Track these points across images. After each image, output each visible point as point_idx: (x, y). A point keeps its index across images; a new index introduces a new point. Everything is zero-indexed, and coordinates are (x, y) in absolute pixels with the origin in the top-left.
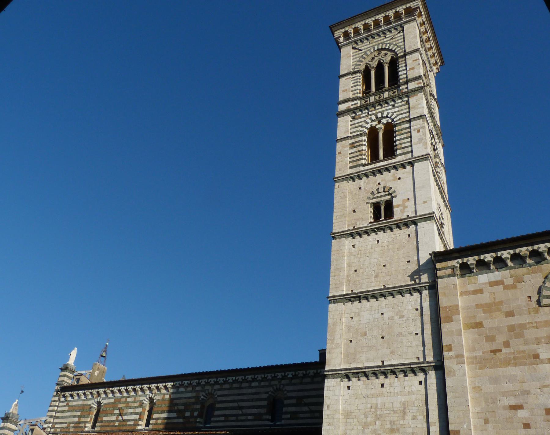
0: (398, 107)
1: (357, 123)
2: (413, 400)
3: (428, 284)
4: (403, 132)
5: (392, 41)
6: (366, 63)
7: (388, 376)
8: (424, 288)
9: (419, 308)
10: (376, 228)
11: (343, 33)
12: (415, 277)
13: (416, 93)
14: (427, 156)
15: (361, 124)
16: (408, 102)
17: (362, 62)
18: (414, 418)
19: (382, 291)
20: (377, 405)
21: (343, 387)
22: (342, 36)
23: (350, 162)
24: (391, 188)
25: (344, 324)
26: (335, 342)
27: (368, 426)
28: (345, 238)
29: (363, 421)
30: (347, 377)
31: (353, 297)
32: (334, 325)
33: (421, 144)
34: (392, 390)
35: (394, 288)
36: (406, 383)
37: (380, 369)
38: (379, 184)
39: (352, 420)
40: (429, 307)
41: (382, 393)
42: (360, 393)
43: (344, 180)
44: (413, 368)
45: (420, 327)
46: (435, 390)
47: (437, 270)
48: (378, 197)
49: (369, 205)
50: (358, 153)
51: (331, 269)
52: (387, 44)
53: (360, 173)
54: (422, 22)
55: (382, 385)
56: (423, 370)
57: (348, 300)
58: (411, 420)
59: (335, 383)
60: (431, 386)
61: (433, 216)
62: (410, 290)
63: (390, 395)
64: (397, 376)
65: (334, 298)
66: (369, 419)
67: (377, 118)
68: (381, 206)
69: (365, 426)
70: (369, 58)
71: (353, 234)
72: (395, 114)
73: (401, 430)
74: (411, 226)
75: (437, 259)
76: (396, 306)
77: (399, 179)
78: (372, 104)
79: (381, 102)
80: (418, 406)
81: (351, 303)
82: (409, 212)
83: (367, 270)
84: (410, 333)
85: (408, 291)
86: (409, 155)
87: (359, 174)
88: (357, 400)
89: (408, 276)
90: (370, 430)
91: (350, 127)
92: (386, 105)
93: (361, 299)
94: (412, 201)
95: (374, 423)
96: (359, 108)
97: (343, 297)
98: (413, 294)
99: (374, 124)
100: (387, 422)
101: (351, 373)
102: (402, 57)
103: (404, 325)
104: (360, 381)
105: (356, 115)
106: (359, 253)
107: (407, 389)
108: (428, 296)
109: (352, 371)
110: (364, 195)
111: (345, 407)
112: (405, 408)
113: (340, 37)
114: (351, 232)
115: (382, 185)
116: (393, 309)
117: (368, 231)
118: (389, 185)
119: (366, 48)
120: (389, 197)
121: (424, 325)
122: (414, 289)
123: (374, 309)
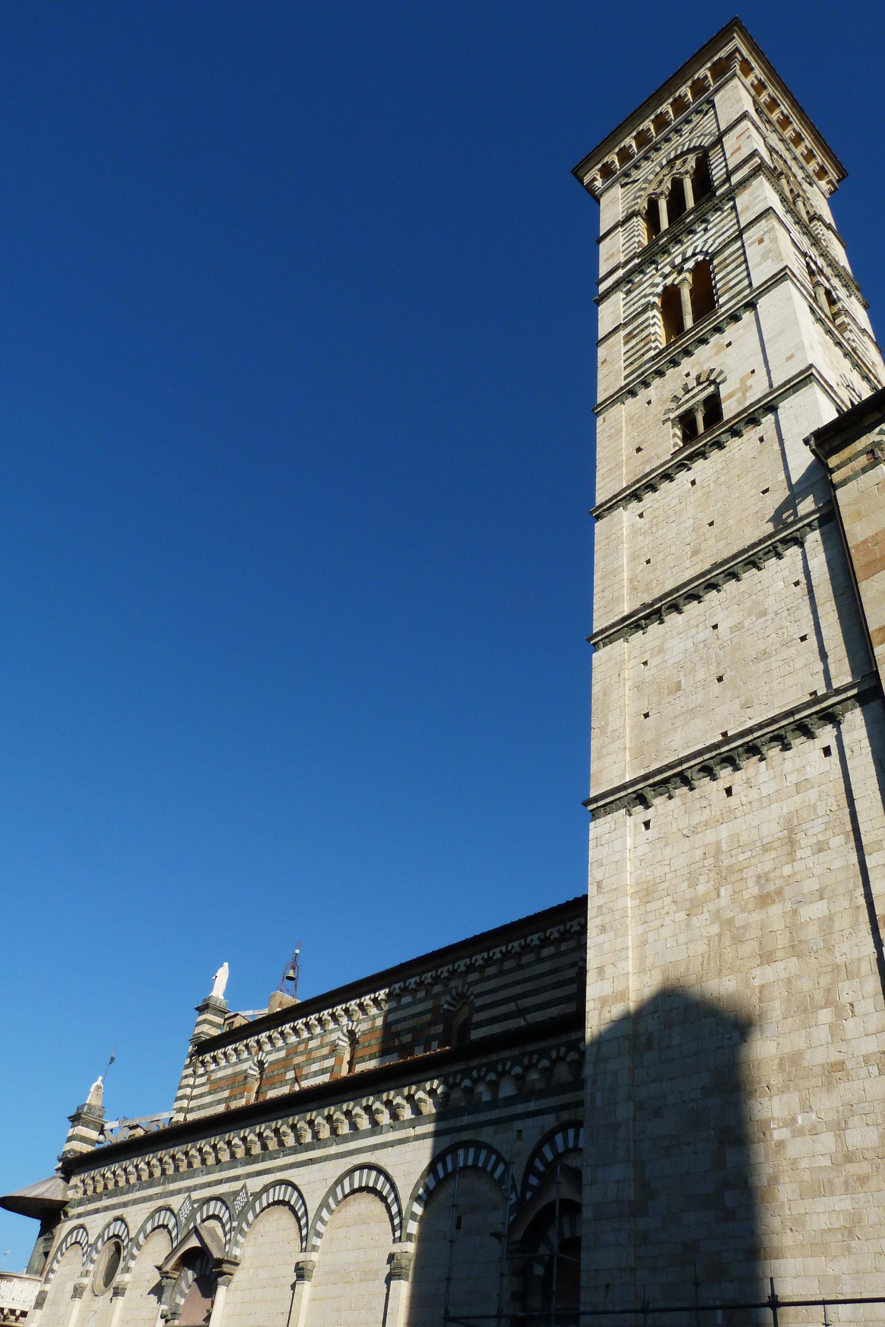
0: (715, 225)
1: (636, 296)
2: (812, 803)
3: (817, 515)
4: (728, 261)
5: (694, 134)
6: (649, 195)
7: (741, 762)
8: (808, 529)
9: (802, 578)
10: (685, 458)
11: (600, 170)
12: (784, 516)
13: (748, 183)
14: (783, 273)
15: (643, 293)
16: (734, 208)
17: (640, 197)
18: (820, 848)
19: (709, 577)
20: (718, 844)
21: (633, 829)
22: (598, 177)
23: (625, 368)
24: (712, 370)
25: (628, 684)
26: (610, 729)
27: (700, 907)
28: (622, 508)
29: (688, 896)
30: (642, 800)
31: (646, 617)
32: (606, 693)
33: (770, 260)
34: (754, 794)
35: (735, 557)
36: (788, 766)
37: (718, 752)
38: (688, 375)
39: (659, 904)
40: (825, 563)
41: (730, 811)
42: (675, 829)
43: (613, 403)
44: (803, 720)
45: (809, 620)
46: (868, 753)
47: (831, 471)
48: (687, 401)
49: (670, 423)
50: (642, 344)
51: (595, 580)
52: (684, 145)
53: (645, 375)
54: (756, 82)
55: (729, 791)
56: (831, 717)
57: (634, 628)
58: (813, 855)
59: (613, 823)
60: (855, 749)
61: (812, 374)
62: (775, 548)
63: (751, 809)
64: (762, 754)
65: (603, 636)
66: (701, 889)
67: (674, 267)
68: (696, 414)
69: (693, 907)
70: (654, 185)
71: (638, 492)
72: (710, 241)
73: (788, 893)
74: (763, 420)
75: (827, 447)
76: (746, 596)
77: (729, 344)
78: (663, 248)
79: (679, 236)
80: (828, 812)
81: (641, 632)
82: (758, 389)
83: (673, 550)
84: (785, 644)
85: (770, 551)
86: (748, 291)
87: (643, 377)
88: (668, 849)
89: (767, 522)
90: (706, 915)
91: (622, 310)
92: (691, 236)
93: (664, 614)
94: (761, 372)
95: (714, 895)
96: (637, 268)
97: (622, 626)
98: (784, 552)
99: (669, 281)
101: (650, 786)
102: (713, 145)
103: (770, 631)
104: (673, 800)
105: (633, 283)
106: (654, 524)
107: (793, 778)
108: (820, 542)
109: (651, 781)
110: (657, 409)
111: (641, 876)
112: (791, 831)
113: (595, 179)
114: (634, 488)
115: (693, 375)
116: (739, 605)
117: (670, 471)
118: (707, 367)
119: (646, 173)
120: (712, 388)
121: (819, 609)
122: (784, 541)
123: (695, 624)
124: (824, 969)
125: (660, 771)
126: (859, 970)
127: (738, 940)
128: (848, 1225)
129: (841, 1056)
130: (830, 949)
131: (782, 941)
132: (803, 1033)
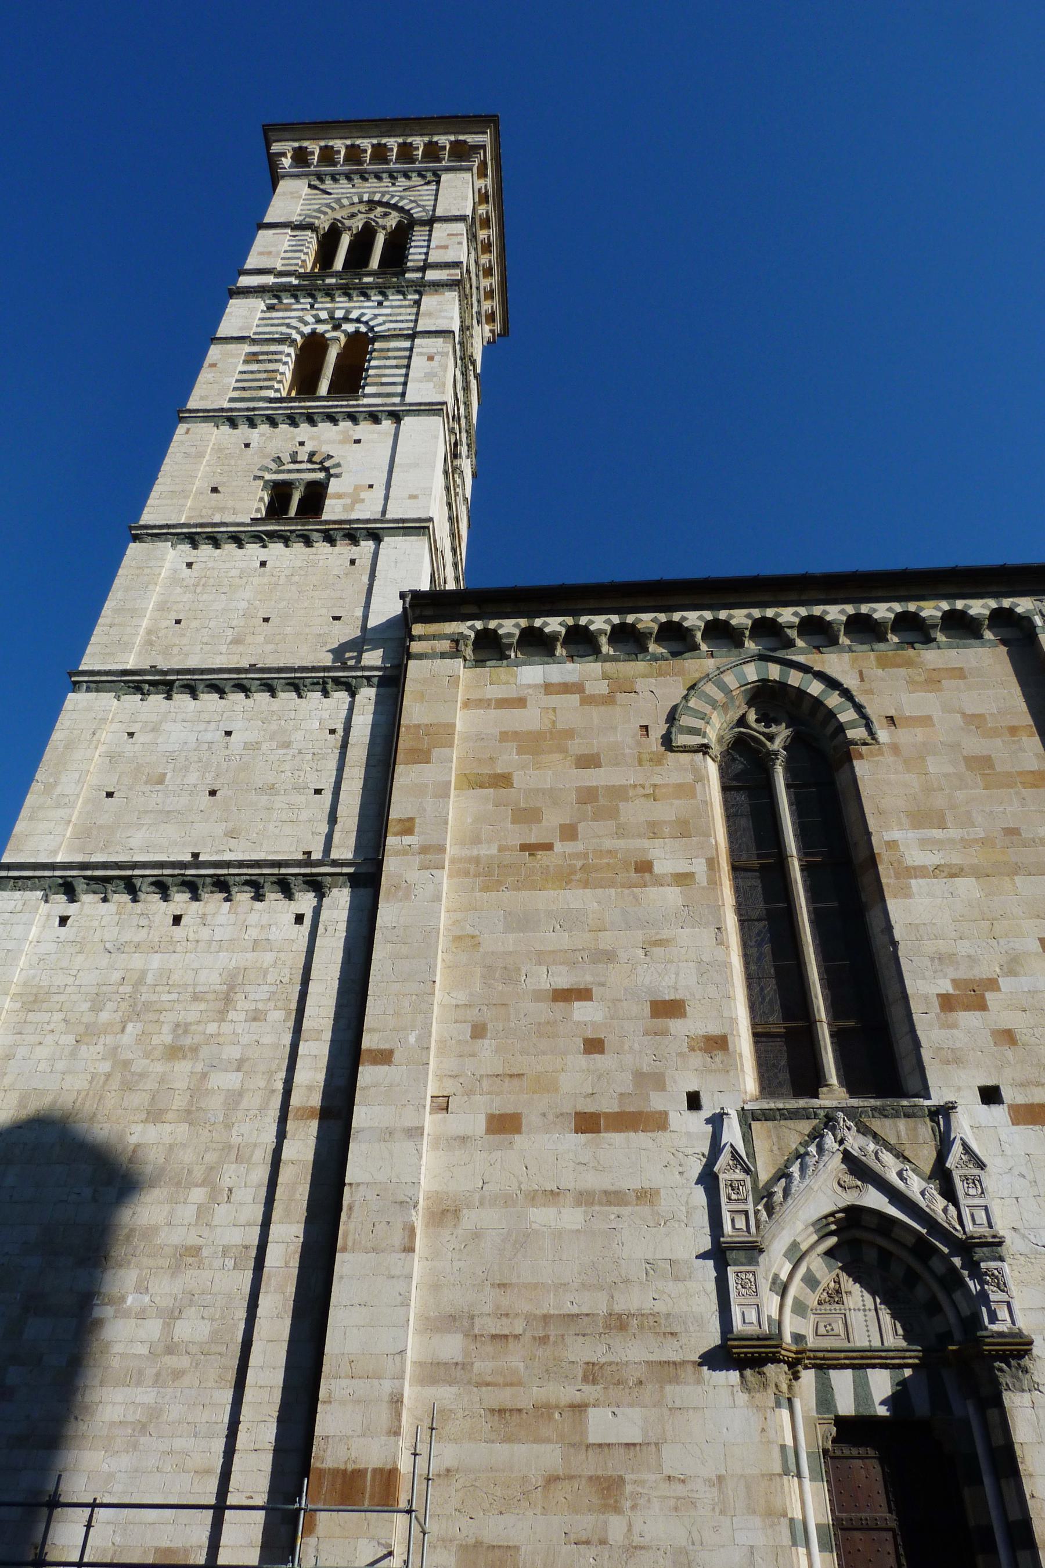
0: (392, 307)
1: (278, 318)
2: (264, 966)
3: (380, 673)
4: (390, 354)
5: (408, 193)
6: (335, 219)
7: (203, 894)
8: (365, 681)
9: (340, 728)
10: (266, 533)
11: (294, 149)
12: (348, 655)
13: (441, 289)
14: (439, 407)
15: (287, 321)
16: (417, 303)
17: (325, 213)
18: (257, 1016)
19: (243, 676)
20: (144, 973)
21: (44, 918)
22: (289, 155)
23: (235, 389)
24: (330, 457)
25: (102, 749)
26: (59, 790)
27: (96, 1037)
28: (170, 543)
29: (85, 1020)
30: (69, 891)
31: (152, 683)
32: (70, 745)
33: (431, 385)
34: (205, 933)
35: (280, 670)
36: (253, 918)
37: (182, 872)
38: (302, 444)
39: (46, 1017)
40: (370, 726)
41: (171, 942)
42: (97, 937)
43: (206, 419)
44: (288, 877)
45: (331, 776)
46: (341, 938)
47: (412, 638)
48: (290, 471)
49: (261, 483)
50: (264, 376)
51: (105, 609)
52: (393, 196)
53: (256, 413)
54: (483, 191)
55: (177, 920)
56: (317, 886)
57: (133, 688)
58: (245, 1021)
59: (21, 903)
60: (329, 929)
61: (428, 528)
62: (325, 683)
63: (195, 949)
64: (230, 895)
65: (91, 679)
66: (104, 1016)
67: (332, 318)
68: (294, 491)
69: (87, 1034)
70: (345, 213)
71: (197, 537)
72: (380, 319)
73: (204, 1052)
74: (362, 543)
75: (418, 612)
76: (275, 718)
77: (358, 441)
78: (329, 289)
79: (350, 289)
80: (278, 982)
81: (140, 696)
82: (368, 509)
83: (212, 624)
84: (298, 789)
85: (318, 683)
86: (397, 400)
87: (252, 413)
88: (80, 958)
89: (328, 651)
90: (100, 1048)
91: (257, 322)
92: (362, 299)
93: (175, 690)
94: (379, 492)
95: (118, 1028)
96: (292, 289)
97: (119, 679)
98: (332, 693)
99: (321, 328)
100: (165, 1025)
101: (85, 877)
102: (423, 223)
103: (287, 766)
104: (106, 904)
105: (281, 302)
106: (202, 583)
107: (253, 933)
108: (373, 701)
109: (89, 873)
110: (253, 460)
111: (34, 977)
112: (232, 988)
113: (284, 154)
114: (194, 530)
115: (308, 447)
116: (264, 723)
117: (242, 536)
118: (326, 449)
119: (343, 193)
120: (321, 475)
121: (346, 769)
122: (337, 681)
123: (207, 720)
124: (214, 1145)
125: (105, 866)
126: (252, 1156)
127: (127, 1087)
128: (144, 1420)
129: (200, 1242)
130: (228, 1126)
131: (179, 1102)
132: (167, 1208)
